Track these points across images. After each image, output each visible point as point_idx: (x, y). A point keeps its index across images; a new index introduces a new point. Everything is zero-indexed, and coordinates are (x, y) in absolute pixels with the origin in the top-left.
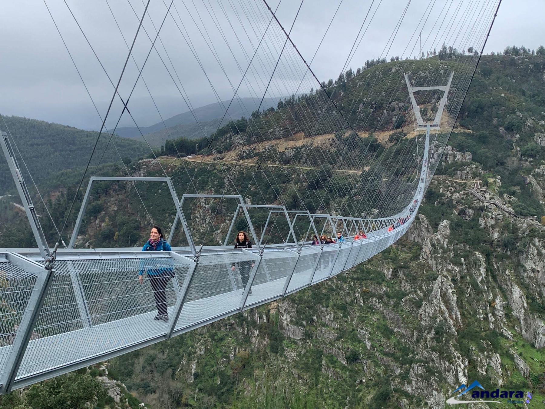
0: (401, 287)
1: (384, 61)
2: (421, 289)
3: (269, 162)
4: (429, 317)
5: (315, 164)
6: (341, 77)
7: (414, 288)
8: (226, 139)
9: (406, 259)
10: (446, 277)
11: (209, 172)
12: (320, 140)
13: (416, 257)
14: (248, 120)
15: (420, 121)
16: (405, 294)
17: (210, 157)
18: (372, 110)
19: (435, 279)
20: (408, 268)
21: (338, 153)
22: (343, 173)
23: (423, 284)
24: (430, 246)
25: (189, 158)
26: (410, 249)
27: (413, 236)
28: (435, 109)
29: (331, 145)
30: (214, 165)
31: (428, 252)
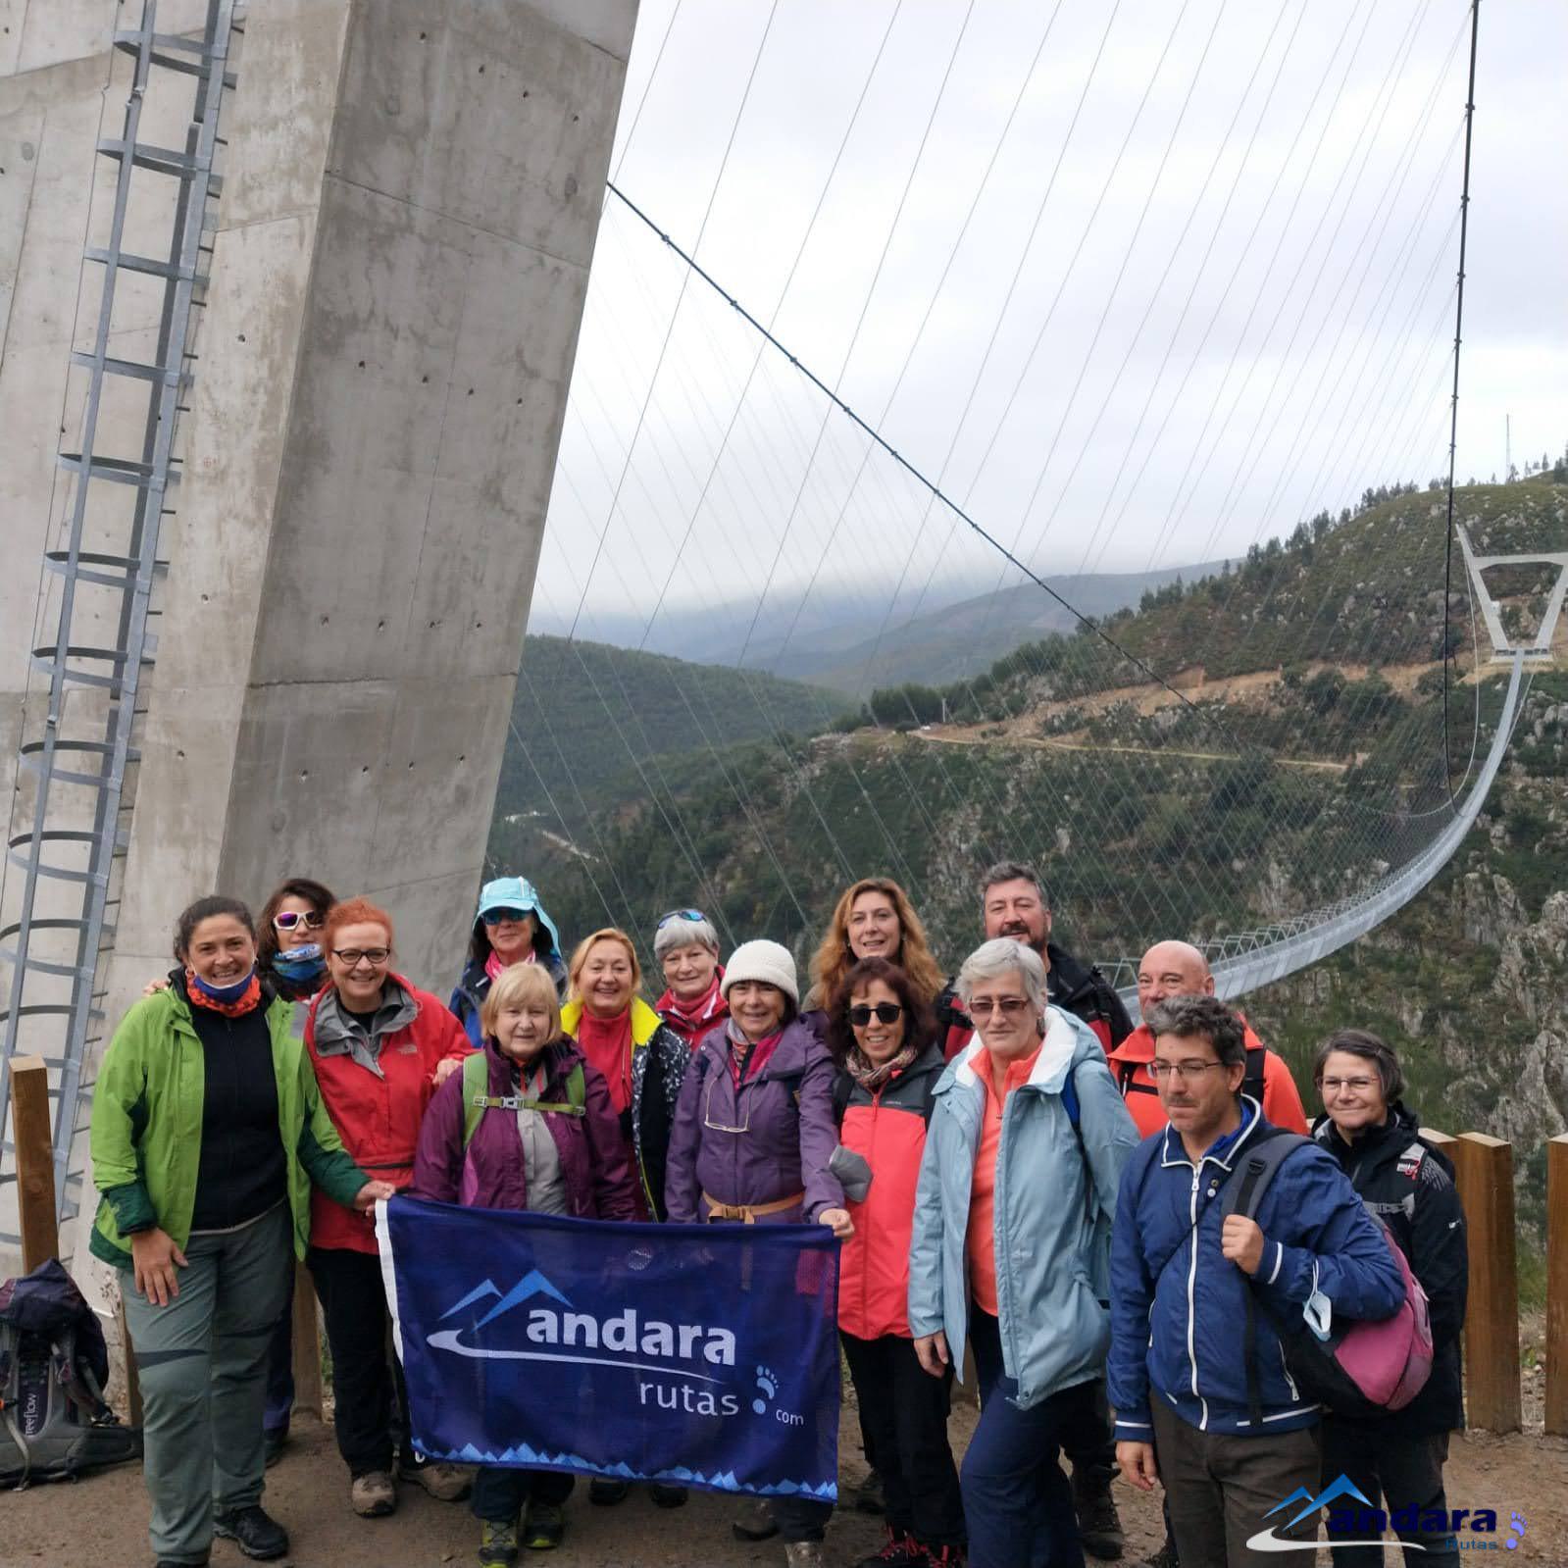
0: (1444, 1055)
2: (1495, 1062)
3: (1116, 741)
4: (1515, 1132)
5: (1227, 745)
6: (1299, 534)
7: (1479, 1061)
8: (1013, 685)
9: (1459, 986)
10: (1559, 1034)
11: (969, 765)
12: (1244, 688)
13: (1484, 983)
14: (1065, 638)
15: (1499, 638)
16: (1454, 1075)
17: (972, 730)
18: (1377, 612)
19: (1531, 1039)
20: (1463, 1009)
21: (1292, 719)
22: (1303, 768)
23: (1500, 1053)
24: (1519, 955)
25: (924, 733)
26: (1469, 961)
27: (1478, 930)
28: (1539, 610)
30: (982, 750)
31: (1515, 971)
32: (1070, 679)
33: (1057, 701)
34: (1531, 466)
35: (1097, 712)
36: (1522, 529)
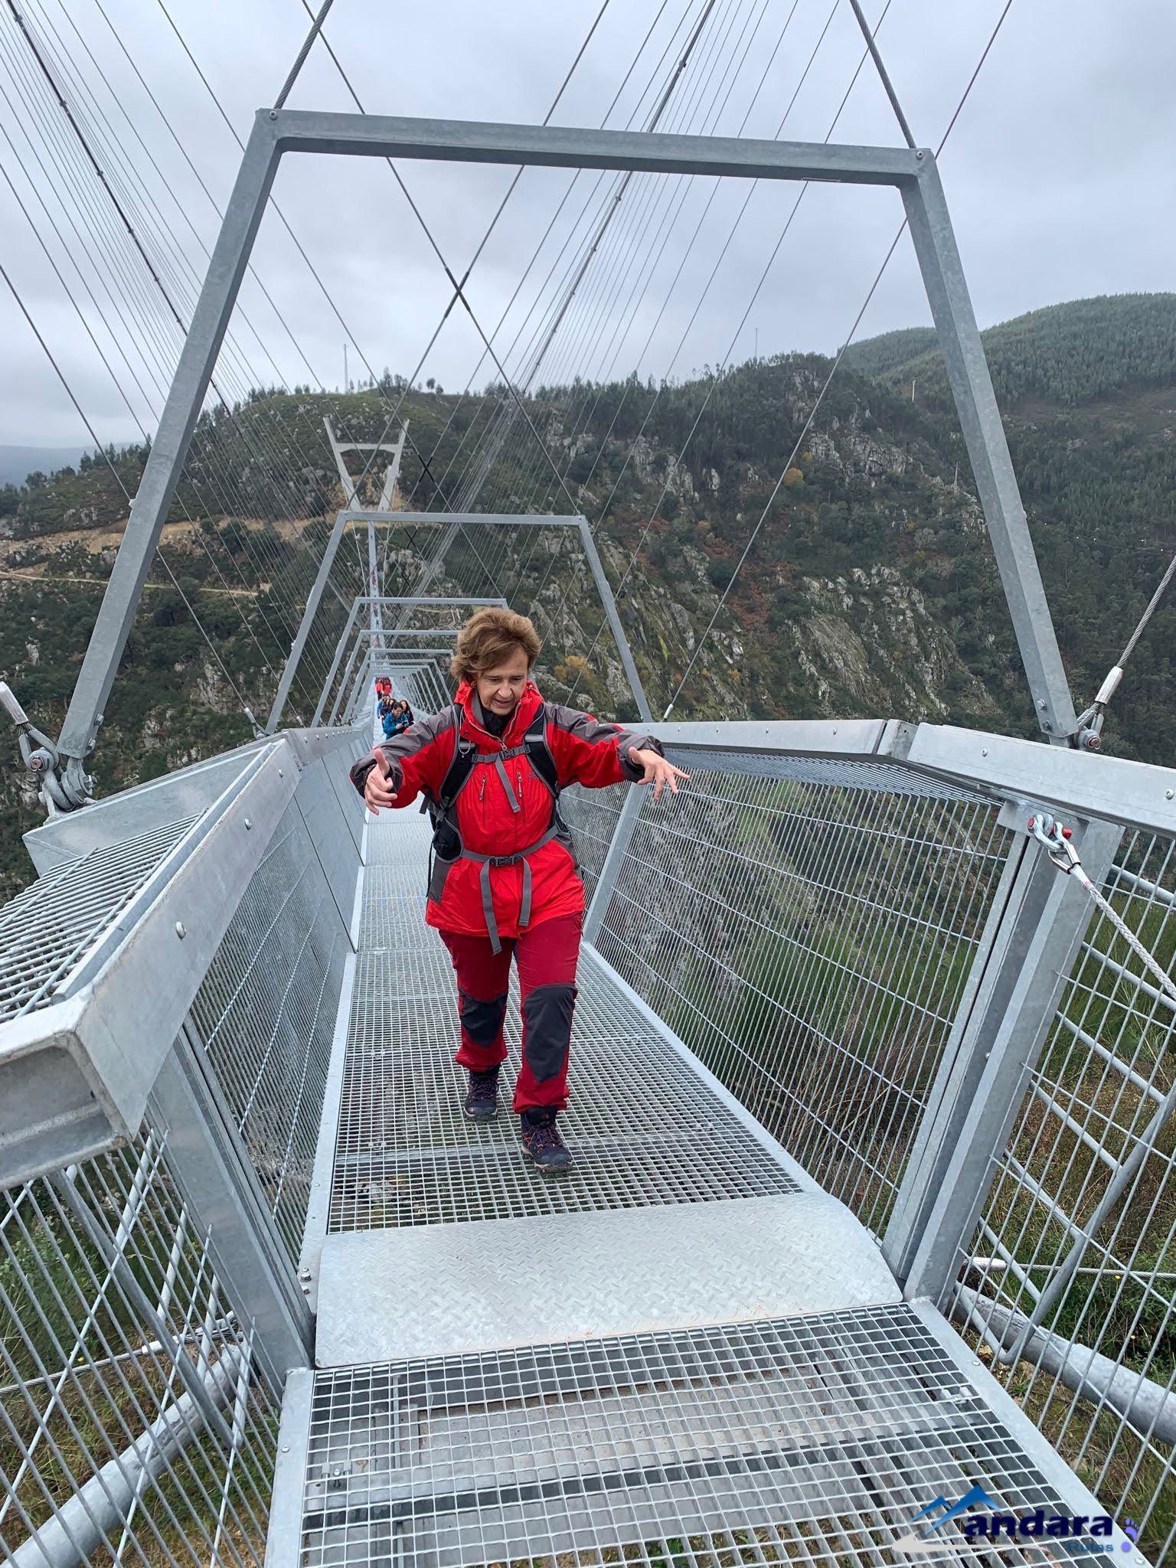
1: (282, 393)
3: (71, 573)
14: (19, 489)
22: (222, 594)
28: (379, 485)
29: (194, 542)
32: (26, 522)
33: (18, 540)
34: (362, 383)
35: (53, 551)
36: (362, 427)
